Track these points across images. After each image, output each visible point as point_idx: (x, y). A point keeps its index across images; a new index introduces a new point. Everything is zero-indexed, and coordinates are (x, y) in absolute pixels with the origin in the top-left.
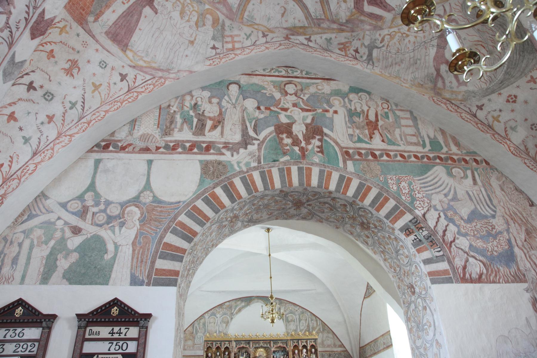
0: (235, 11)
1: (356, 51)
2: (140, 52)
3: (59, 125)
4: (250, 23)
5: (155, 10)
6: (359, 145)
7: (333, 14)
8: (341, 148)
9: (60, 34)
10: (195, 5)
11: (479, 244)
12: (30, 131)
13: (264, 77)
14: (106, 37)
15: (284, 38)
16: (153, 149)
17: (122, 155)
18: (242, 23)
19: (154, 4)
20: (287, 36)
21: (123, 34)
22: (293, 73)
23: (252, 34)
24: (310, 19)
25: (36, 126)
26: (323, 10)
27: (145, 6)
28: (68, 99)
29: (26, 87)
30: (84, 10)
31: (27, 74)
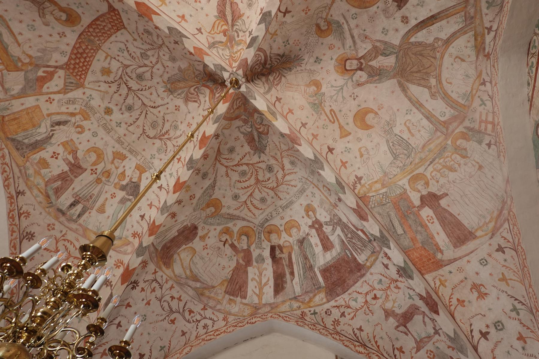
0: (457, 113)
2: (480, 222)
3: (531, 335)
4: (470, 98)
5: (444, 195)
7: (459, 2)
9: (445, 287)
10: (446, 154)
13: (536, 88)
14: (458, 248)
15: (487, 60)
18: (469, 107)
19: (439, 194)
20: (485, 56)
21: (459, 232)
22: (535, 47)
23: (481, 97)
24: (466, 29)
25: (523, 356)
26: (455, 14)
27: (439, 204)
28: (508, 311)
29: (483, 338)
30: (430, 260)
31: (471, 331)
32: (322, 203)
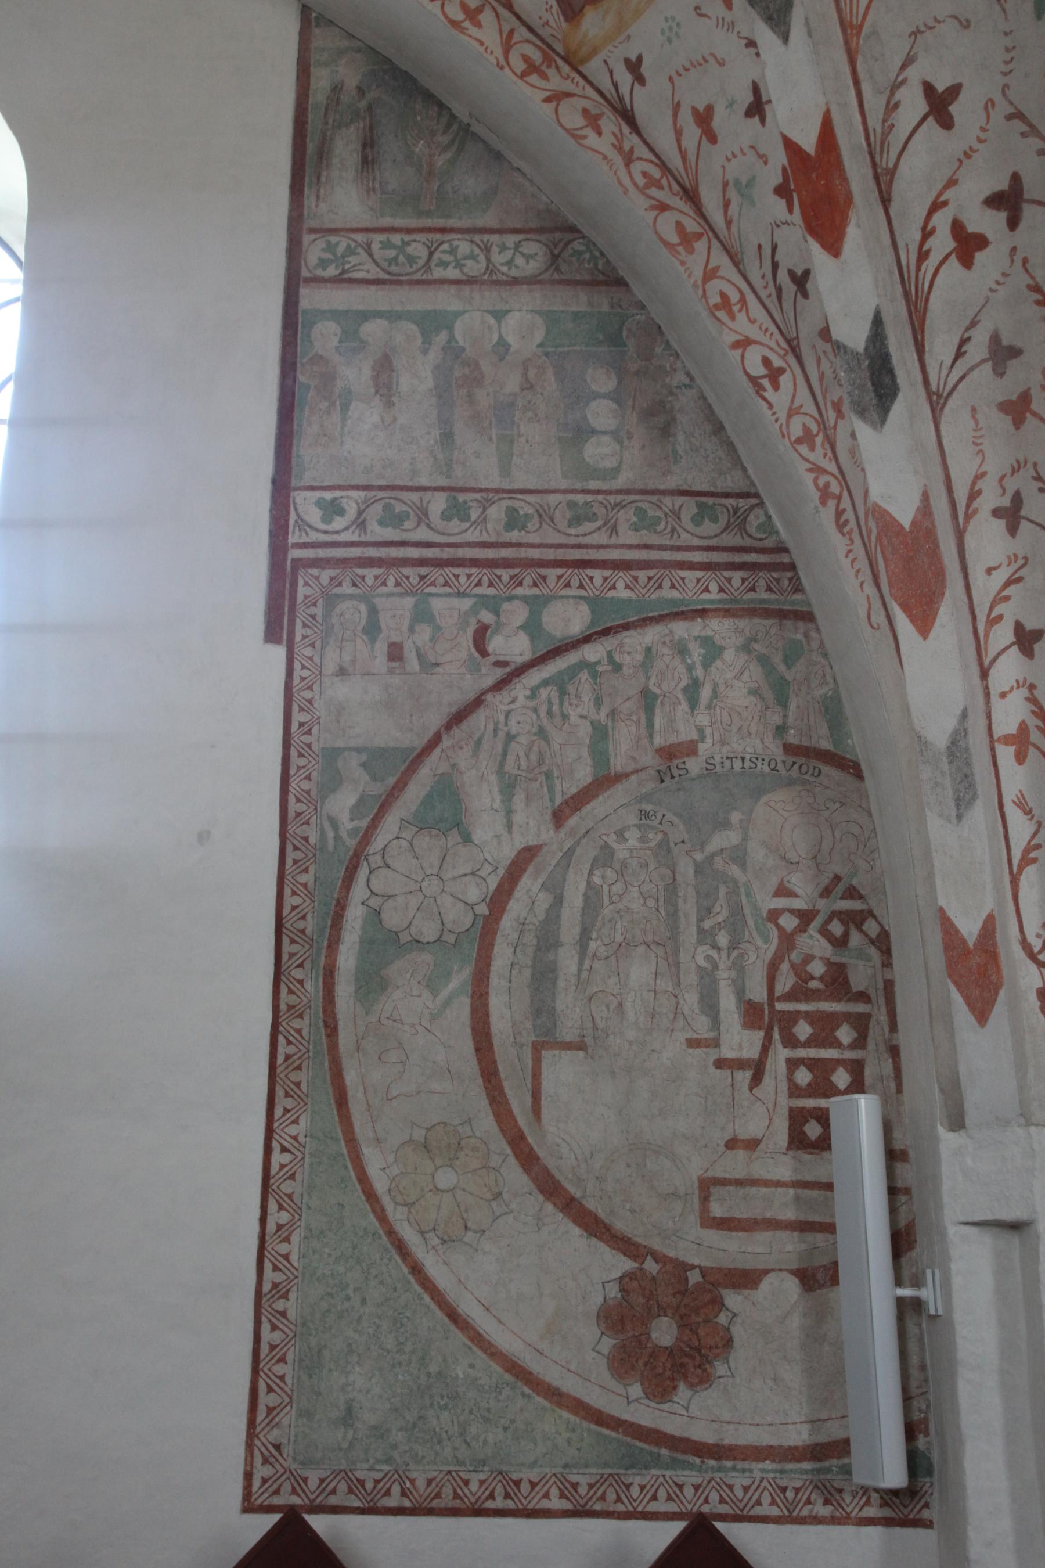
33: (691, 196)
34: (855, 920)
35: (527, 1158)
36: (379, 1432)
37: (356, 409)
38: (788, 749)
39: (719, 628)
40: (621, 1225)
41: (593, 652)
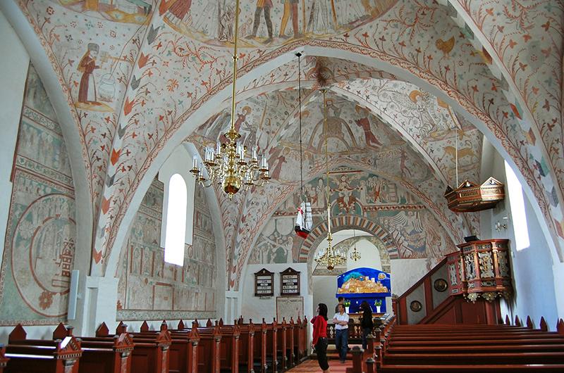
1: (369, 161)
6: (370, 204)
8: (362, 206)
11: (412, 244)
12: (255, 217)
16: (293, 213)
17: (283, 217)
32: (257, 117)
33: (84, 136)
34: (72, 245)
35: (34, 275)
36: (12, 315)
37: (28, 143)
38: (70, 219)
39: (65, 197)
40: (43, 285)
41: (51, 197)
